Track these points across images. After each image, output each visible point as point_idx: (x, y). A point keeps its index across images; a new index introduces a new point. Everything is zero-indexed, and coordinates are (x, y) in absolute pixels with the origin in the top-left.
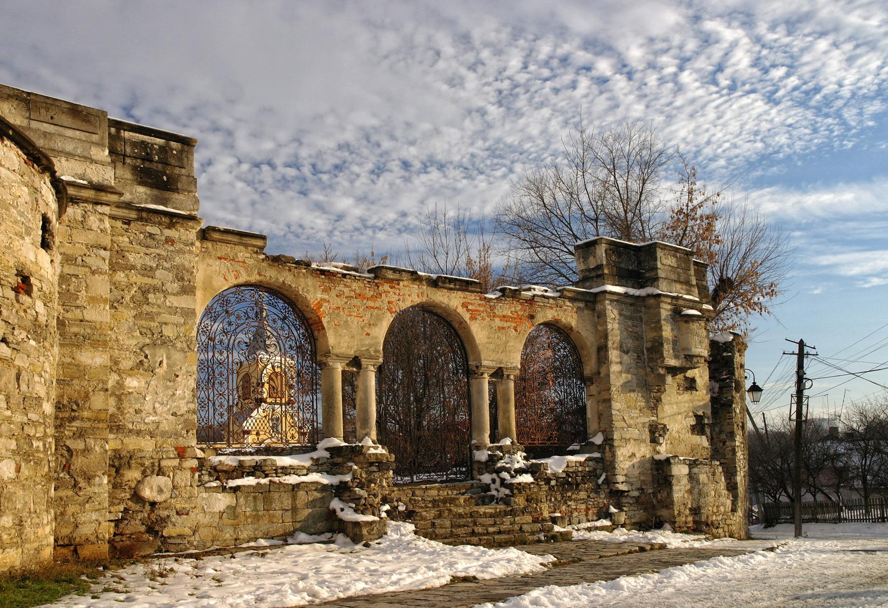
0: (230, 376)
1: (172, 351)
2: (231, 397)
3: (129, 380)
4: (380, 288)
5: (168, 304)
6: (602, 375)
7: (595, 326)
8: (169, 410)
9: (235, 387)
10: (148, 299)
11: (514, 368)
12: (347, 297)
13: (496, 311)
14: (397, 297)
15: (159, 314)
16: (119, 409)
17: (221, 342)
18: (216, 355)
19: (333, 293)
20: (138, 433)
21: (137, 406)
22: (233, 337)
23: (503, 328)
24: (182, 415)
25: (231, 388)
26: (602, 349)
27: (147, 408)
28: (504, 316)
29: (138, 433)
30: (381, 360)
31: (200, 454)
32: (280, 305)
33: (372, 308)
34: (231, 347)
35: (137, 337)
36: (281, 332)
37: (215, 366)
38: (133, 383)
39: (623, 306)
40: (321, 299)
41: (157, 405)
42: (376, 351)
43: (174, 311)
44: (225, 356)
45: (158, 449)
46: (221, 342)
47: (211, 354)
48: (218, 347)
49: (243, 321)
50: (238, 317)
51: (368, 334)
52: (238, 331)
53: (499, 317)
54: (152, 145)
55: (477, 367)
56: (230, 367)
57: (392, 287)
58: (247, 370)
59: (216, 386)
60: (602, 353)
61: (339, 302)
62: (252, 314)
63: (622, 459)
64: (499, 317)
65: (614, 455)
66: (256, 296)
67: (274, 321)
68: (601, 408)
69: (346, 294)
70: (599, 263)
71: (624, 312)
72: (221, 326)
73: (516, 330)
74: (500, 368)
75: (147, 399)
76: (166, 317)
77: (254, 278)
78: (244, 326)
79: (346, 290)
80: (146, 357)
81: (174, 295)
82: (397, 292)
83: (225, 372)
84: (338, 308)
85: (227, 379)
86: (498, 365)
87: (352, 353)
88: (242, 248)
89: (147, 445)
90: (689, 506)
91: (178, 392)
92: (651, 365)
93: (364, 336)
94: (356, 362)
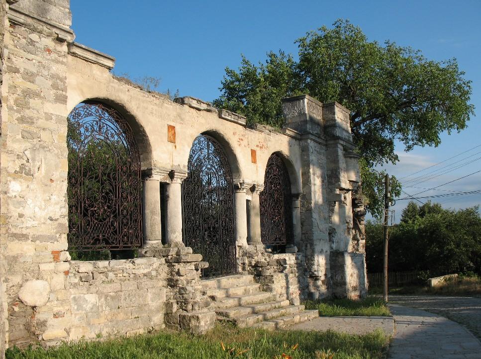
7: (302, 156)
15: (38, 118)
20: (23, 237)
21: (21, 210)
24: (56, 220)
29: (23, 237)
30: (187, 175)
38: (15, 187)
39: (316, 144)
42: (184, 166)
43: (48, 117)
50: (87, 130)
55: (241, 184)
68: (303, 217)
71: (316, 149)
74: (254, 185)
75: (28, 202)
76: (41, 122)
77: (102, 94)
80: (28, 161)
86: (253, 183)
87: (169, 168)
89: (27, 249)
90: (352, 285)
92: (330, 187)
94: (171, 175)
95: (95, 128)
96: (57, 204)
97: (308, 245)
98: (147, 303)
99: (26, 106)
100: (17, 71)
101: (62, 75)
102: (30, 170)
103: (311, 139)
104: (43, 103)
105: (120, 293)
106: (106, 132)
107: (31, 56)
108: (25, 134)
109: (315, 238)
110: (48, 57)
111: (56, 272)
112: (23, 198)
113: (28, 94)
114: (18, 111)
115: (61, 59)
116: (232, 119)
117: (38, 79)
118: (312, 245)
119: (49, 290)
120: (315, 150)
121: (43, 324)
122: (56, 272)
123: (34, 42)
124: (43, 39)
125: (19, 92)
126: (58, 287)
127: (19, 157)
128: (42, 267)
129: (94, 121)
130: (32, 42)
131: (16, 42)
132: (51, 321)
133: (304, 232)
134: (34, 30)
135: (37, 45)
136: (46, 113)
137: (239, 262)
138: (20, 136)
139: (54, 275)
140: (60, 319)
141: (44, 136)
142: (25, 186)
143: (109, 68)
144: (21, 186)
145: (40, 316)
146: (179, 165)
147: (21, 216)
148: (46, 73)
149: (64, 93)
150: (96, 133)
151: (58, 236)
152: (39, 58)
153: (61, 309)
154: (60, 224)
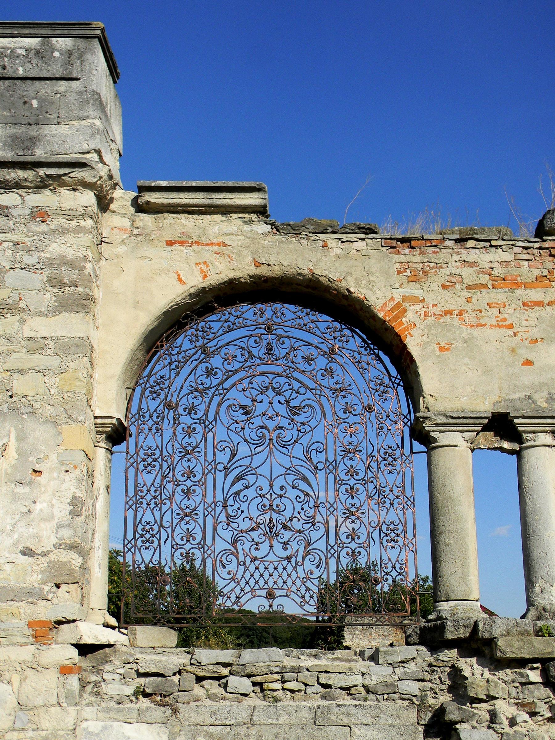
0: (210, 478)
1: (30, 424)
2: (210, 520)
9: (219, 497)
12: (469, 288)
18: (179, 437)
19: (435, 281)
22: (217, 399)
25: (209, 500)
31: (93, 631)
32: (322, 326)
34: (211, 417)
40: (404, 299)
44: (199, 437)
46: (191, 410)
47: (168, 433)
49: (238, 365)
52: (227, 385)
56: (210, 458)
58: (247, 462)
59: (178, 497)
61: (453, 300)
66: (269, 313)
67: (309, 359)
69: (468, 281)
78: (242, 374)
84: (449, 312)
85: (202, 483)
93: (519, 368)
95: (255, 352)
105: (243, 730)
111: (35, 666)
126: (39, 701)
129: (251, 336)
143: (261, 211)
150: (258, 361)
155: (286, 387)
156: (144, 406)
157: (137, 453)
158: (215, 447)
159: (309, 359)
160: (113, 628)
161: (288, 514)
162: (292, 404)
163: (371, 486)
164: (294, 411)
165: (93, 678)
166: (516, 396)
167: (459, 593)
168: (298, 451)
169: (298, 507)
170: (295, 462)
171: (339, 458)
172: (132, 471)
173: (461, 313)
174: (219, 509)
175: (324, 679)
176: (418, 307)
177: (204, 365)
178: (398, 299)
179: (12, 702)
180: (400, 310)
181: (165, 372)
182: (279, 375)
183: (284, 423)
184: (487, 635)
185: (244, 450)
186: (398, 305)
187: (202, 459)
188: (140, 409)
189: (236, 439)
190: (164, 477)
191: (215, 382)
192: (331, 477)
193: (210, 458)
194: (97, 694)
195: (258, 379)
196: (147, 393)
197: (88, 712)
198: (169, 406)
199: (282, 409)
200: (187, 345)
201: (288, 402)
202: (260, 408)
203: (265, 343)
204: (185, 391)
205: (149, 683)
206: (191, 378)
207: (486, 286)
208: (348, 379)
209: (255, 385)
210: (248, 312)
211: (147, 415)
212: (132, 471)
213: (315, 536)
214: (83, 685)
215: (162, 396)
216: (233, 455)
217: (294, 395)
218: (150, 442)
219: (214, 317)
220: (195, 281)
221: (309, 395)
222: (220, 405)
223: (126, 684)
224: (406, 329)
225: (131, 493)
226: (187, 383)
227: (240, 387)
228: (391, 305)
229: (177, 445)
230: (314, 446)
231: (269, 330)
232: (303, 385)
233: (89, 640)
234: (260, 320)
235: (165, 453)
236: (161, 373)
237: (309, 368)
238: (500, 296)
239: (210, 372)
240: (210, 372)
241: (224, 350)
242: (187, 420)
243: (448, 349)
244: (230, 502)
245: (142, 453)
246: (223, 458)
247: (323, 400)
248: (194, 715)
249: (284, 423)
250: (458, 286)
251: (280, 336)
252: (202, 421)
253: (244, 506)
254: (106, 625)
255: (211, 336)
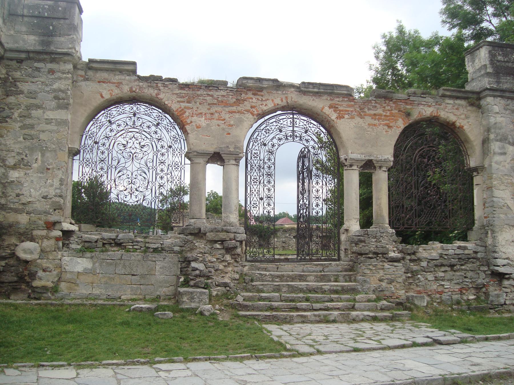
0: (110, 170)
3: (12, 172)
4: (243, 95)
5: (46, 117)
6: (486, 166)
8: (41, 194)
9: (113, 178)
10: (31, 114)
11: (385, 161)
13: (366, 110)
14: (260, 103)
15: (39, 124)
16: (3, 193)
17: (104, 145)
18: (99, 155)
20: (16, 211)
21: (18, 191)
23: (375, 125)
24: (50, 199)
25: (109, 178)
26: (485, 142)
27: (25, 193)
28: (375, 115)
31: (67, 226)
33: (235, 112)
35: (20, 142)
36: (154, 136)
37: (98, 163)
38: (14, 175)
39: (509, 101)
40: (185, 108)
41: (32, 190)
43: (49, 122)
45: (30, 222)
46: (104, 145)
48: (102, 148)
49: (122, 128)
51: (229, 134)
52: (117, 136)
53: (370, 115)
54: (44, 5)
55: (346, 160)
56: (110, 163)
57: (254, 94)
58: (123, 165)
60: (486, 146)
61: (203, 109)
62: (130, 123)
63: (503, 243)
64: (370, 115)
65: (494, 238)
66: (135, 108)
67: (149, 127)
68: (485, 196)
69: (209, 102)
70: (483, 63)
72: (104, 132)
73: (389, 127)
78: (123, 132)
79: (208, 98)
80: (26, 156)
81: (51, 110)
82: (260, 98)
83: (105, 168)
84: (201, 113)
86: (367, 158)
87: (212, 149)
88: (118, 73)
89: (23, 219)
91: (49, 181)
96: (52, 186)
97: (489, 233)
98: (153, 272)
99: (29, 116)
100: (22, 92)
101: (63, 87)
102: (28, 162)
103: (494, 96)
104: (44, 113)
106: (141, 125)
107: (34, 80)
108: (26, 136)
109: (496, 223)
110: (53, 77)
112: (20, 183)
113: (29, 108)
114: (21, 121)
115: (65, 75)
116: (322, 90)
117: (40, 95)
118: (493, 232)
119: (40, 250)
120: (505, 109)
121: (33, 276)
122: (47, 238)
123: (39, 68)
124: (47, 65)
125: (23, 107)
127: (19, 154)
128: (35, 233)
130: (38, 69)
131: (23, 72)
132: (40, 273)
133: (485, 215)
134: (39, 61)
135: (42, 70)
136: (47, 119)
137: (342, 247)
138: (21, 139)
139: (45, 240)
140: (48, 273)
141: (42, 136)
142: (22, 174)
144: (19, 173)
145: (33, 269)
146: (228, 147)
147: (18, 195)
148: (47, 89)
149: (65, 101)
151: (51, 211)
152: (42, 80)
153: (50, 266)
154: (54, 203)
155: (140, 137)
156: (86, 142)
157: (83, 160)
158: (112, 159)
159: (149, 127)
160: (73, 224)
161: (138, 185)
162: (142, 144)
163: (169, 176)
164: (142, 147)
165: (67, 242)
166: (223, 146)
167: (198, 216)
168: (143, 162)
169: (142, 183)
170: (141, 166)
171: (158, 165)
172: (81, 167)
173: (205, 114)
174: (113, 182)
175: (147, 245)
176: (190, 111)
177: (109, 128)
178: (183, 107)
179: (39, 250)
180: (183, 112)
181: (95, 130)
182: (137, 132)
183: (138, 151)
184: (203, 232)
185: (122, 161)
186: (183, 110)
187: (107, 163)
188: (85, 144)
189: (120, 156)
190: (92, 170)
191: (113, 134)
192: (154, 172)
193: (110, 163)
194: (68, 248)
195: (130, 134)
196: (88, 138)
197: (65, 254)
198: (96, 143)
199: (138, 146)
200: (103, 120)
201: (140, 143)
202: (129, 145)
203: (133, 120)
204: (102, 137)
205: (87, 245)
206: (104, 132)
207: (216, 104)
208: (163, 135)
209: (128, 136)
210: (127, 107)
211: (87, 146)
212: (81, 167)
213: (148, 193)
214: (64, 245)
215: (93, 139)
216: (118, 163)
217: (142, 140)
218: (88, 156)
219: (114, 109)
220: (107, 96)
221: (148, 140)
222: (114, 143)
223: (79, 244)
224: (185, 119)
225: (81, 175)
226: (103, 135)
227: (122, 136)
228: (180, 109)
229: (98, 158)
230: (149, 160)
231: (135, 115)
232: (147, 137)
233: (65, 229)
234: (131, 111)
235: (93, 161)
236: (93, 130)
237: (149, 130)
238: (219, 109)
239: (111, 131)
240: (111, 131)
241: (117, 122)
242: (102, 148)
243: (200, 127)
244: (117, 180)
245: (85, 160)
246: (115, 163)
247: (153, 143)
248: (102, 256)
249: (138, 151)
250: (205, 104)
251: (139, 118)
252: (108, 149)
253: (122, 182)
254: (71, 223)
255: (113, 116)
